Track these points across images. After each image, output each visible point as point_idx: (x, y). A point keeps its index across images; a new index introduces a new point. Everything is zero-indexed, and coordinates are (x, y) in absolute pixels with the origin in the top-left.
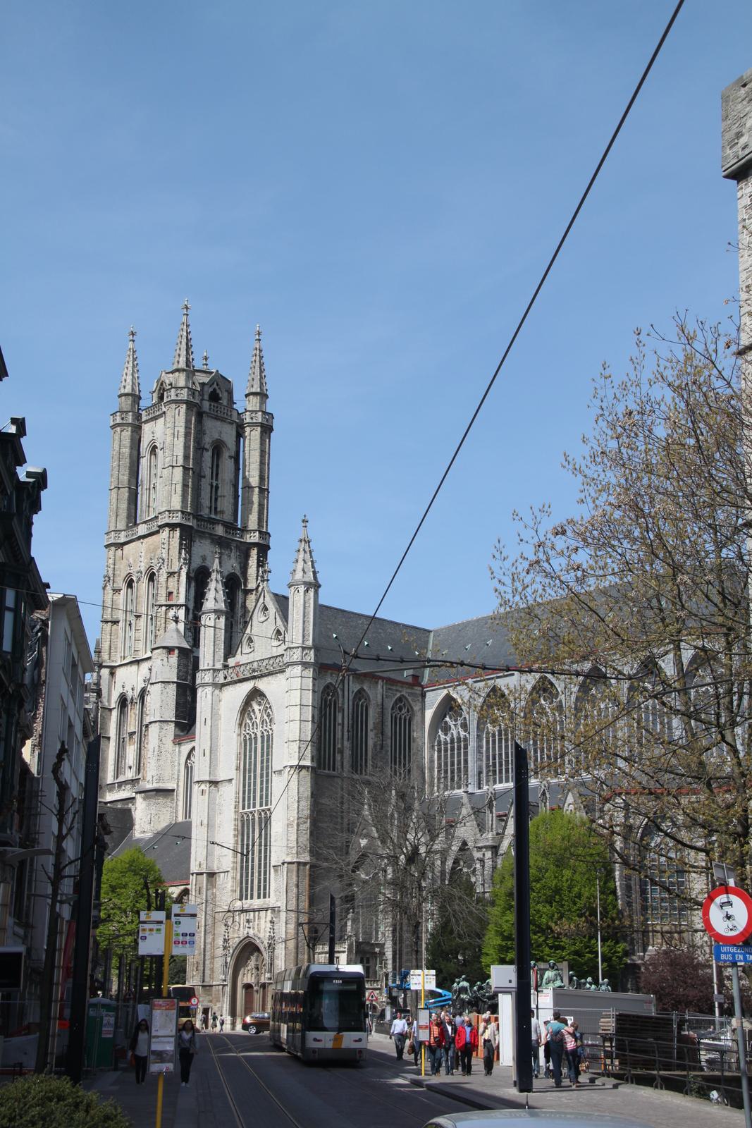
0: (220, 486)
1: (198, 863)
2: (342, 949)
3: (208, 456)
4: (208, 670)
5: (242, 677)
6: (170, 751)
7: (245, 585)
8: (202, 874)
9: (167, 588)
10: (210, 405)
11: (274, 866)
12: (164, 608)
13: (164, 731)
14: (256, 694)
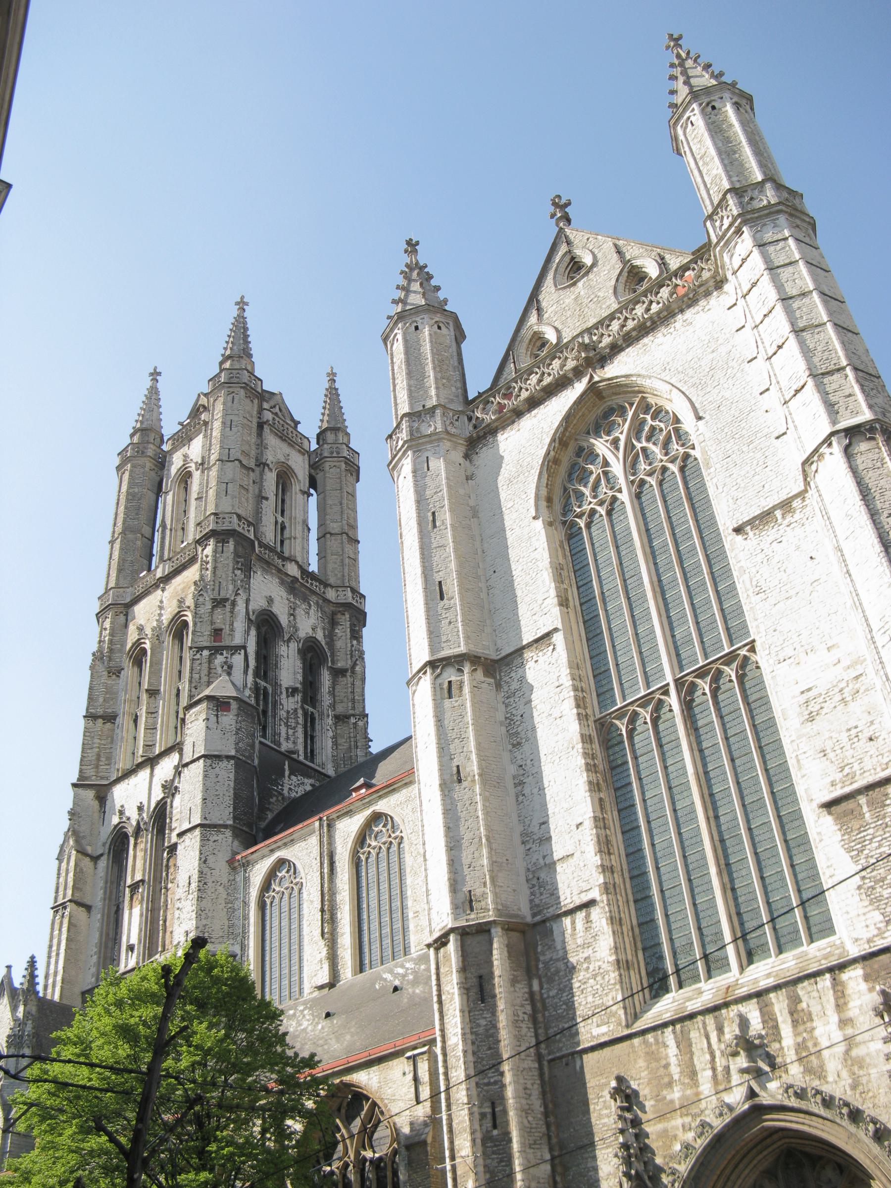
0: (287, 525)
3: (270, 478)
6: (225, 880)
7: (333, 662)
9: (212, 623)
10: (274, 419)
11: (829, 806)
12: (206, 653)
13: (211, 843)
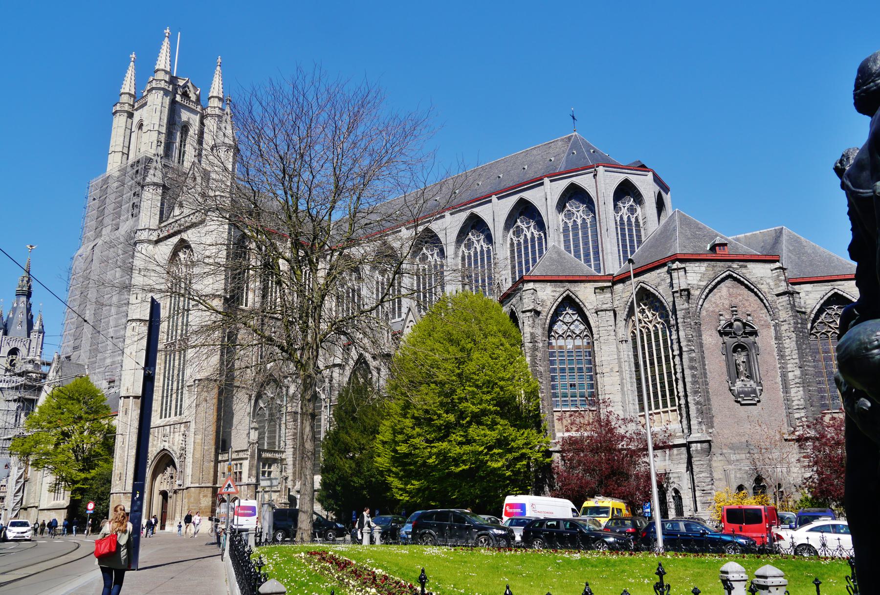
1: (126, 388)
2: (245, 456)
4: (144, 229)
5: (171, 231)
8: (128, 397)
14: (184, 245)
